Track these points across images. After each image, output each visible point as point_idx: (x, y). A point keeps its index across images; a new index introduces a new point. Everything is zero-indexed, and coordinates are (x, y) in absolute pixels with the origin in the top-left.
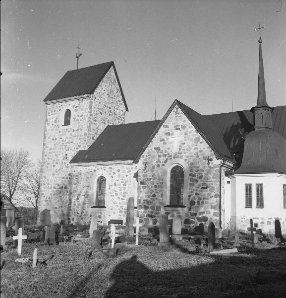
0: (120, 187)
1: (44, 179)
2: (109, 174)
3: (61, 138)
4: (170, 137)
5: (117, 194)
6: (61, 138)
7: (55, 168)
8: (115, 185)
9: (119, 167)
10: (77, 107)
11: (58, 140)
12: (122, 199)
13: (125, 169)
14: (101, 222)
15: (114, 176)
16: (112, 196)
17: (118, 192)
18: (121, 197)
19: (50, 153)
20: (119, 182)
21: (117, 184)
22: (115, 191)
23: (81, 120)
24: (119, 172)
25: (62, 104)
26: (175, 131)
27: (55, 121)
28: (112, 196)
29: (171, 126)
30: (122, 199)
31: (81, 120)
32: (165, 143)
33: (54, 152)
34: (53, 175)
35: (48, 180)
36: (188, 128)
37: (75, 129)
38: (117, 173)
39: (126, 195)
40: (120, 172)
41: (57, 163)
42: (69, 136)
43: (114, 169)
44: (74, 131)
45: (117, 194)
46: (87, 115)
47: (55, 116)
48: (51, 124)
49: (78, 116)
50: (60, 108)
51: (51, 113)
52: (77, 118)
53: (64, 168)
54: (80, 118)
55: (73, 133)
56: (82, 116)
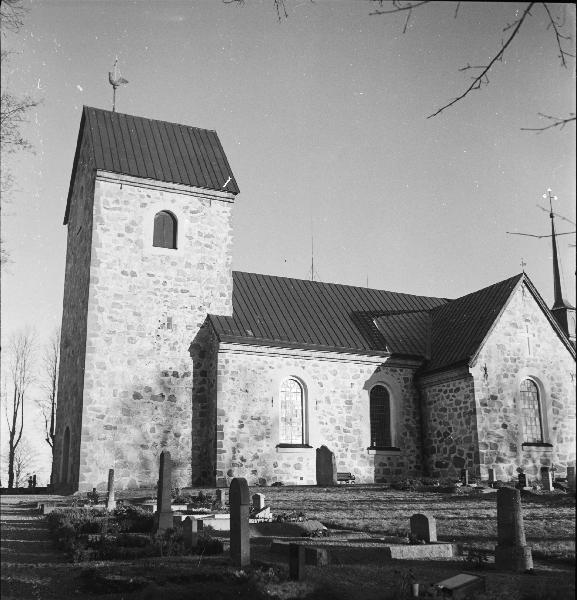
0: (338, 407)
1: (97, 371)
2: (314, 378)
3: (153, 275)
4: (518, 330)
5: (333, 421)
6: (153, 275)
7: (135, 347)
8: (328, 400)
9: (335, 366)
10: (192, 212)
11: (142, 277)
12: (345, 431)
13: (348, 371)
14: (302, 479)
15: (324, 382)
16: (322, 423)
17: (337, 416)
18: (343, 426)
19: (114, 305)
20: (337, 395)
21: (332, 399)
22: (330, 413)
23: (206, 246)
24: (335, 375)
25: (149, 192)
26: (524, 323)
27: (128, 230)
28: (322, 423)
29: (518, 314)
30: (345, 431)
31: (206, 246)
32: (511, 340)
33: (130, 306)
34: (129, 362)
35: (113, 374)
36: (540, 322)
37: (194, 261)
38: (331, 378)
39: (353, 423)
40: (338, 375)
41: (142, 335)
42: (172, 273)
43: (324, 368)
44: (188, 265)
45: (333, 421)
46: (226, 239)
47: (130, 216)
48: (114, 233)
49: (200, 234)
50: (146, 200)
51: (112, 206)
52: (196, 237)
53: (165, 348)
54: (208, 241)
55: (188, 271)
56: (208, 236)
